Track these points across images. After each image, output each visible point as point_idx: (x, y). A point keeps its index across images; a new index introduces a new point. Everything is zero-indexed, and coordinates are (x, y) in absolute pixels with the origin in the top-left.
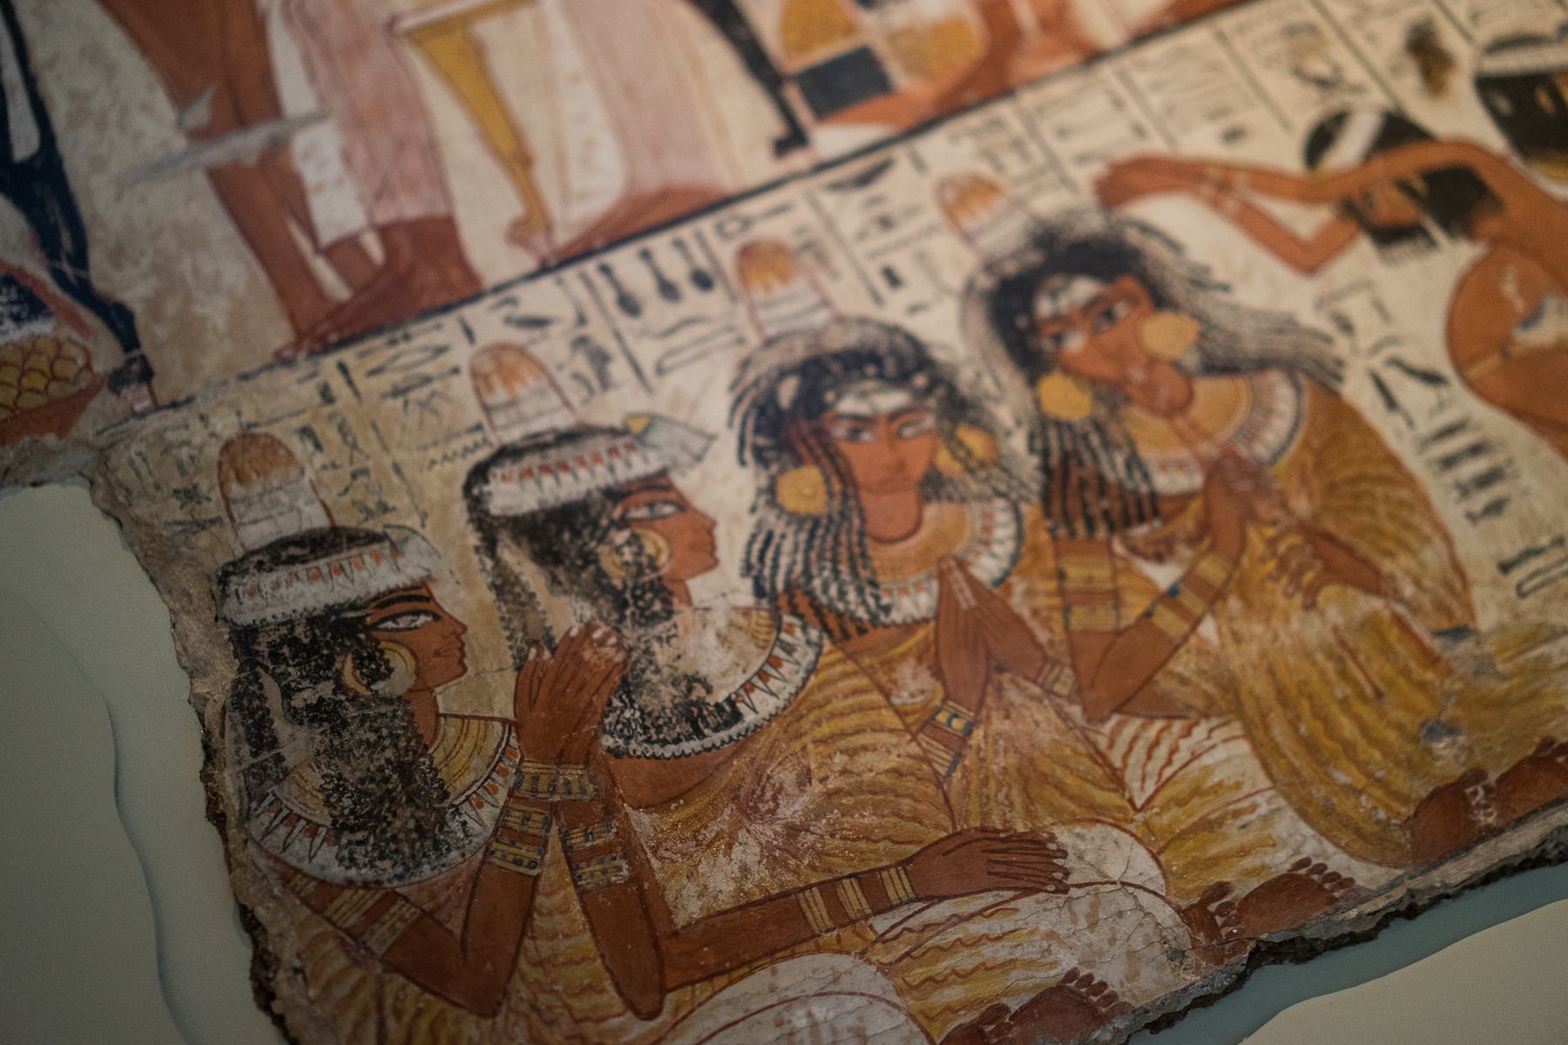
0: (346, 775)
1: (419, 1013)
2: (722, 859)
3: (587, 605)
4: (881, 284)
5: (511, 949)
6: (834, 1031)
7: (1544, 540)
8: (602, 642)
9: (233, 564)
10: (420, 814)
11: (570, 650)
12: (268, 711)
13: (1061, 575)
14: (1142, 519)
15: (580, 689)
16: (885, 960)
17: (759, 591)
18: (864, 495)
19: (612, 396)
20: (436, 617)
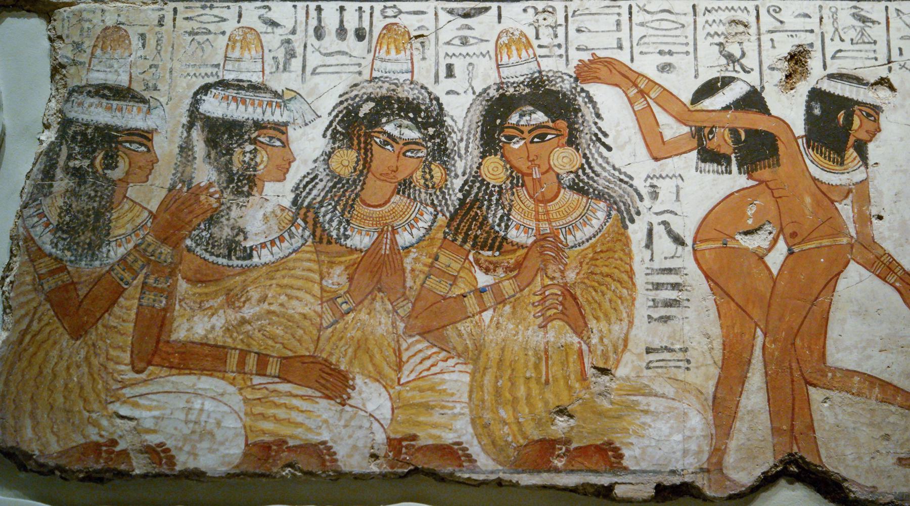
0: (74, 206)
1: (47, 324)
2: (206, 319)
3: (215, 174)
4: (443, 72)
5: (98, 315)
6: (209, 417)
7: (677, 346)
9: (79, 87)
10: (93, 238)
11: (196, 192)
12: (57, 162)
13: (436, 259)
15: (191, 212)
16: (249, 397)
17: (295, 202)
18: (370, 175)
19: (286, 75)
20: (149, 151)
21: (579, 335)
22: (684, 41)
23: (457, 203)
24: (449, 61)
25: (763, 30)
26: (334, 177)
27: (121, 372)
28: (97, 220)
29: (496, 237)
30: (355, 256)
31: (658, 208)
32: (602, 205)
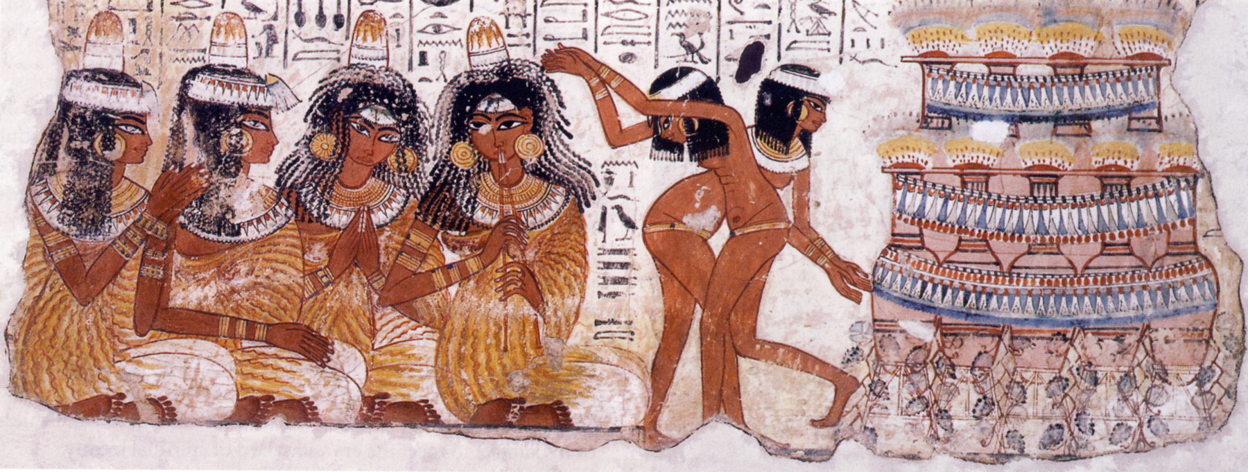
7: (623, 319)
8: (202, 175)
13: (408, 237)
14: (458, 229)
16: (239, 358)
17: (278, 183)
19: (268, 59)
21: (535, 307)
22: (647, 31)
23: (427, 186)
24: (422, 48)
25: (723, 21)
26: (314, 159)
27: (126, 335)
28: (98, 197)
29: (462, 220)
30: (334, 234)
31: (610, 194)
32: (561, 189)
